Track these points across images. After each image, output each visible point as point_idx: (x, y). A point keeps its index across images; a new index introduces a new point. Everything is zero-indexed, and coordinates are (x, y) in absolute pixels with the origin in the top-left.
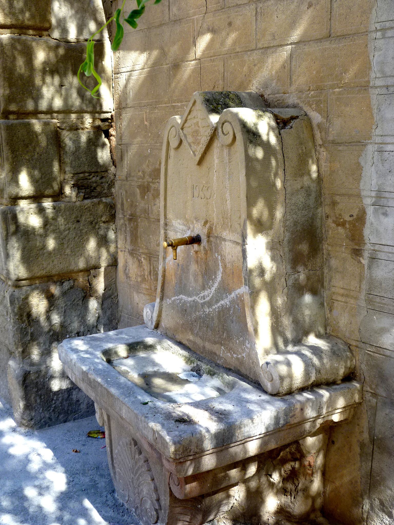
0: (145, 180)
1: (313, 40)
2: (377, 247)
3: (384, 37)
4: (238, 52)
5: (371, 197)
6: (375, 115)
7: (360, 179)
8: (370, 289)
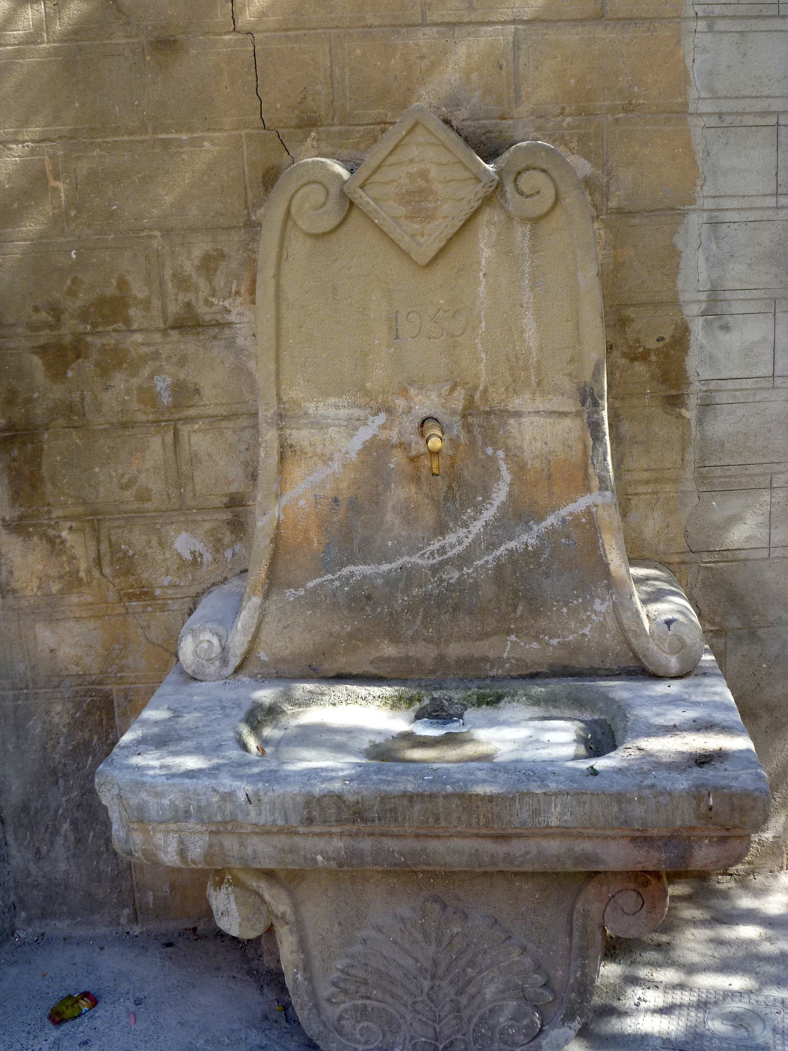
0: (64, 331)
1: (565, 21)
2: (712, 385)
3: (710, 29)
4: (371, 27)
5: (699, 301)
6: (700, 163)
7: (677, 273)
8: (702, 459)
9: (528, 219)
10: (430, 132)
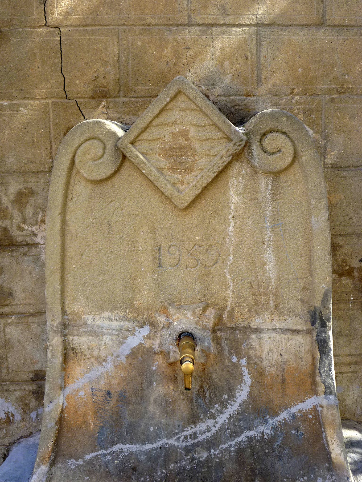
1: (295, 25)
4: (149, 25)
9: (270, 173)
10: (190, 100)
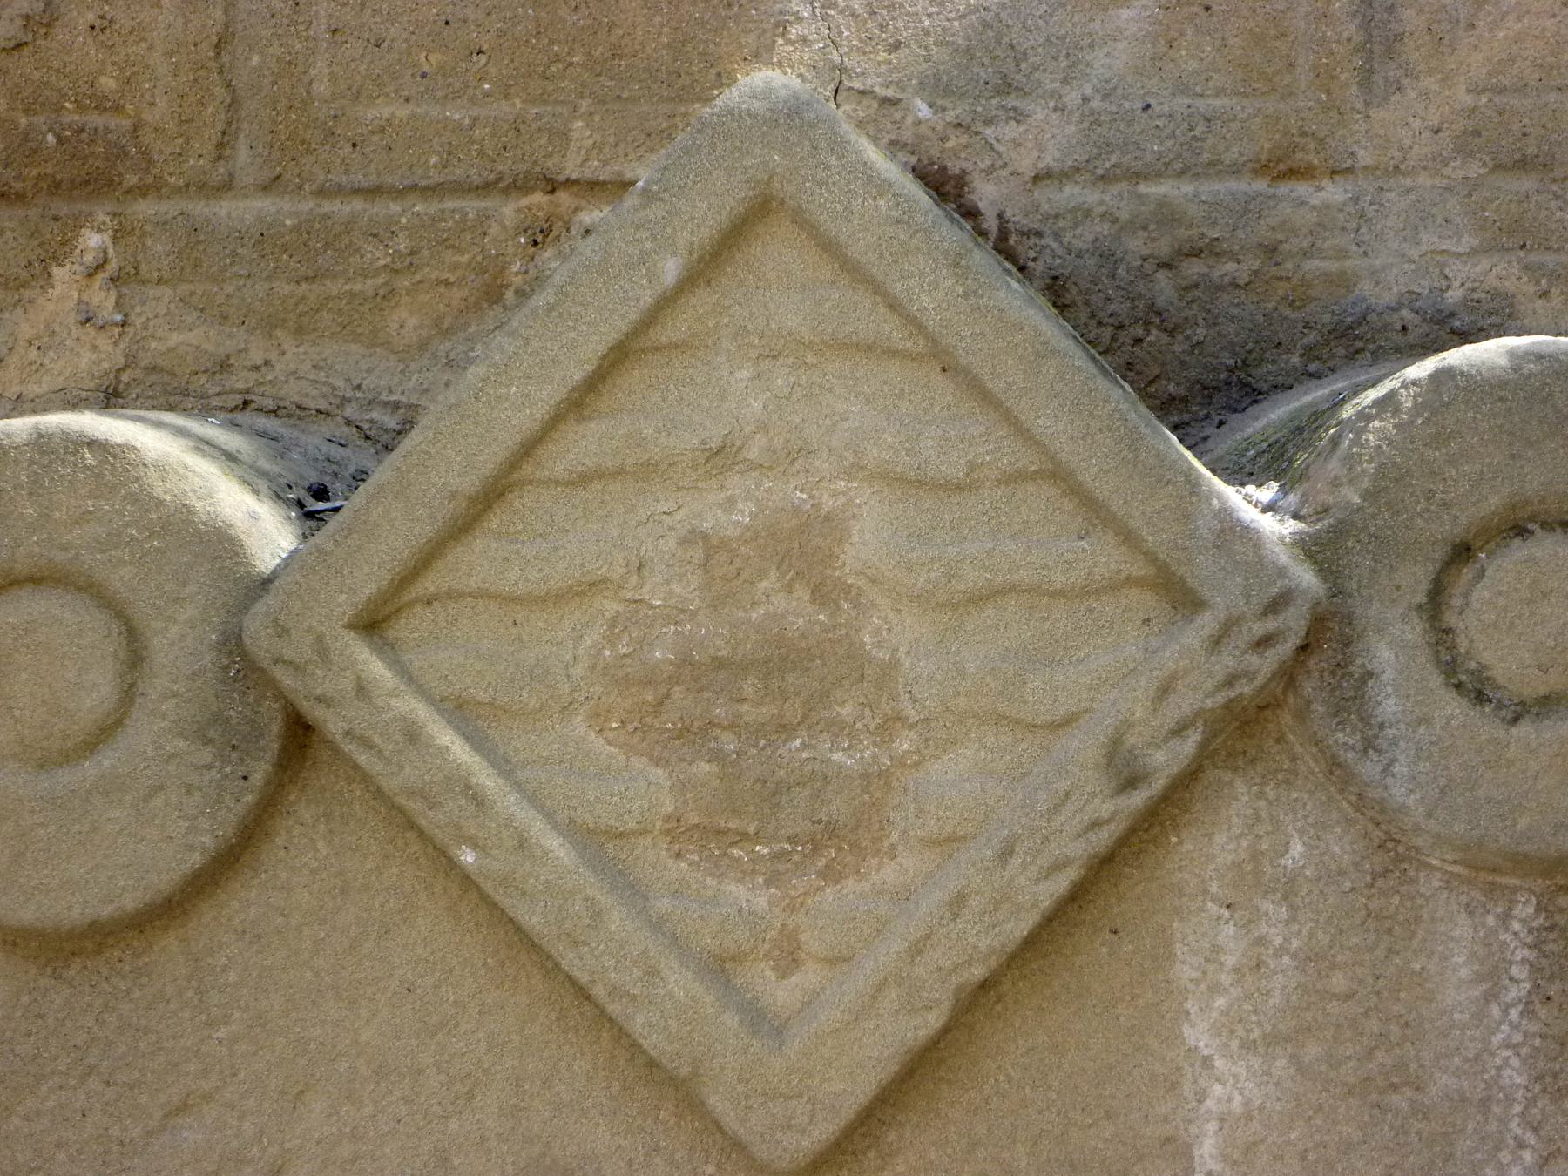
9: (1520, 863)
10: (854, 271)
